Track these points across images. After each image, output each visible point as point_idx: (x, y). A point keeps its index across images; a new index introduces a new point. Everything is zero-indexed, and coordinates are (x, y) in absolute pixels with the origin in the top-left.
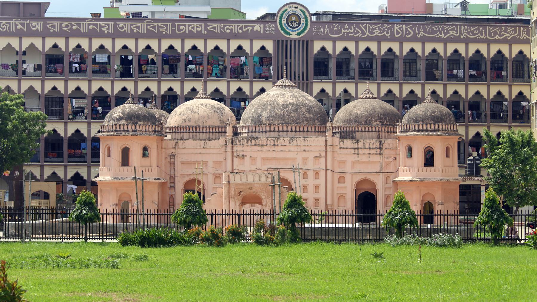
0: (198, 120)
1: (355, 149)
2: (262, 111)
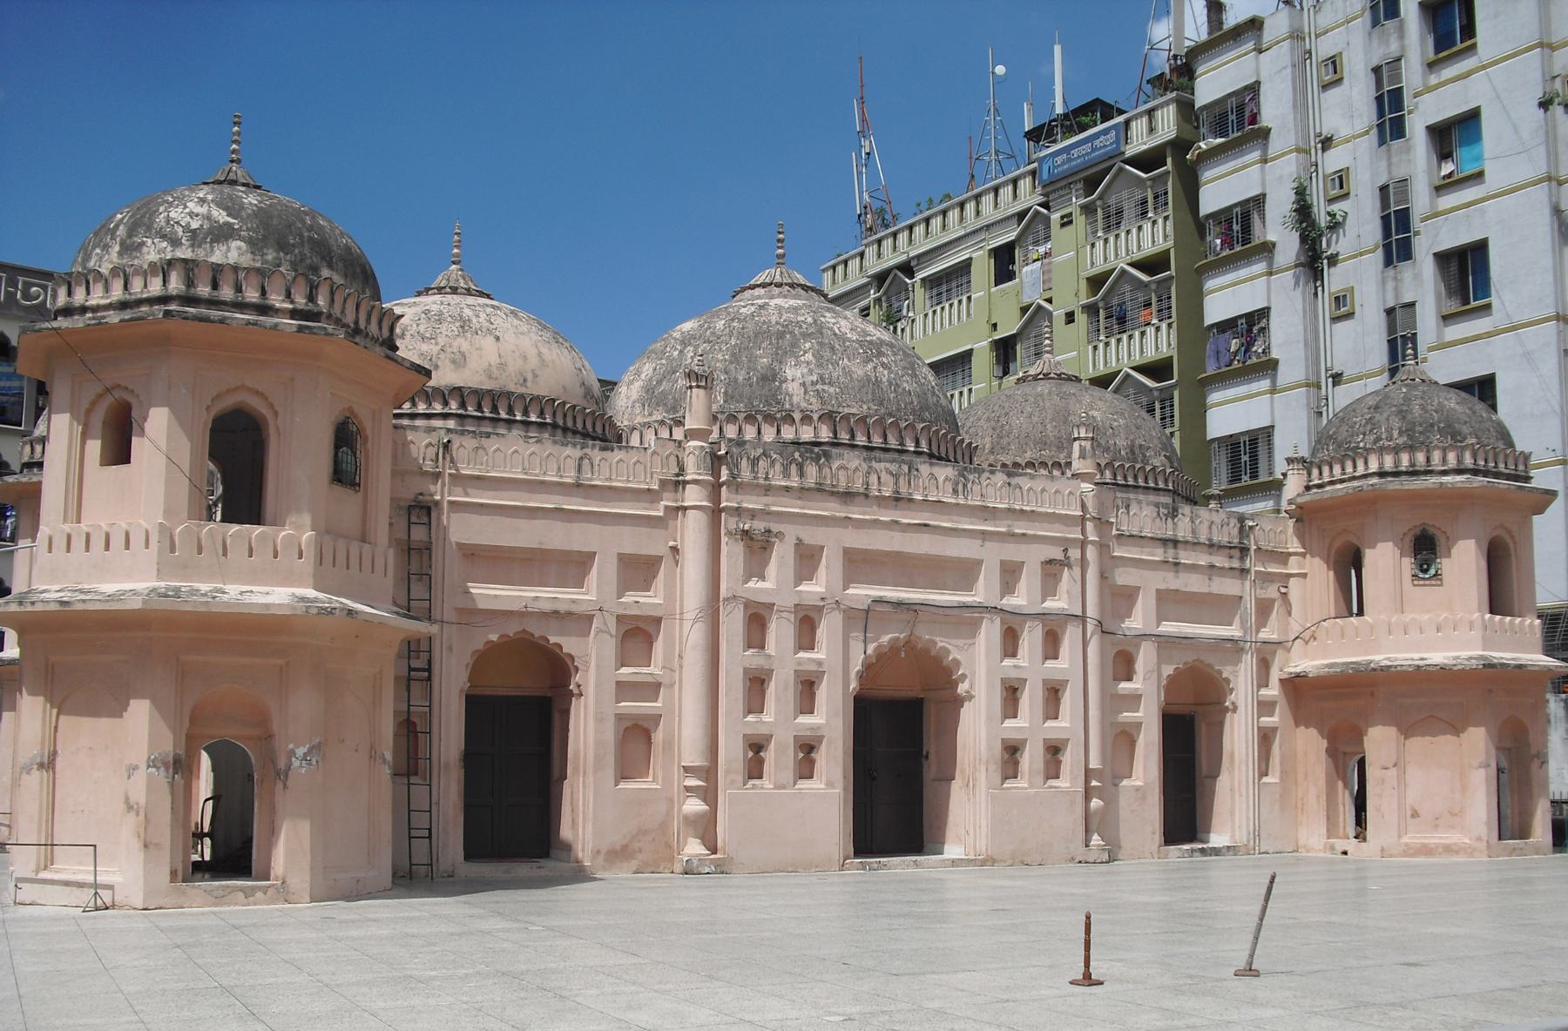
0: (502, 366)
1: (1165, 542)
2: (780, 357)
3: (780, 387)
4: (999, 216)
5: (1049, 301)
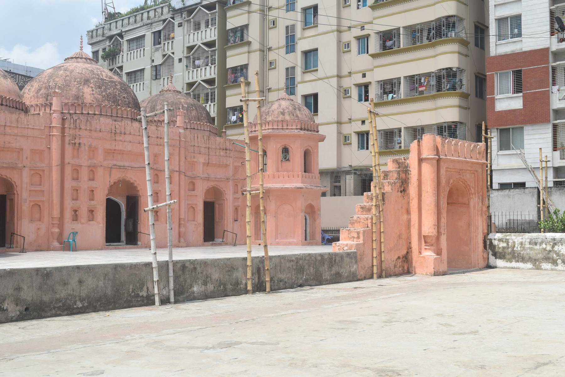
3: (83, 96)
4: (156, 19)
5: (173, 53)
